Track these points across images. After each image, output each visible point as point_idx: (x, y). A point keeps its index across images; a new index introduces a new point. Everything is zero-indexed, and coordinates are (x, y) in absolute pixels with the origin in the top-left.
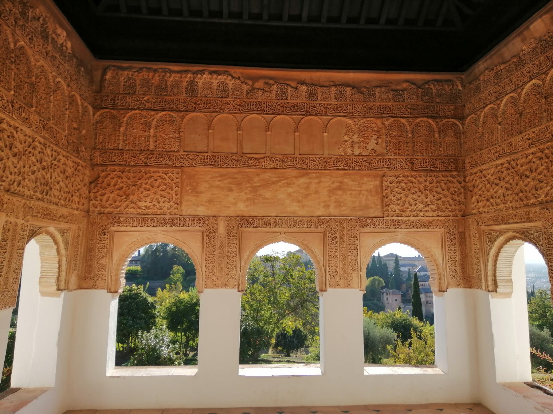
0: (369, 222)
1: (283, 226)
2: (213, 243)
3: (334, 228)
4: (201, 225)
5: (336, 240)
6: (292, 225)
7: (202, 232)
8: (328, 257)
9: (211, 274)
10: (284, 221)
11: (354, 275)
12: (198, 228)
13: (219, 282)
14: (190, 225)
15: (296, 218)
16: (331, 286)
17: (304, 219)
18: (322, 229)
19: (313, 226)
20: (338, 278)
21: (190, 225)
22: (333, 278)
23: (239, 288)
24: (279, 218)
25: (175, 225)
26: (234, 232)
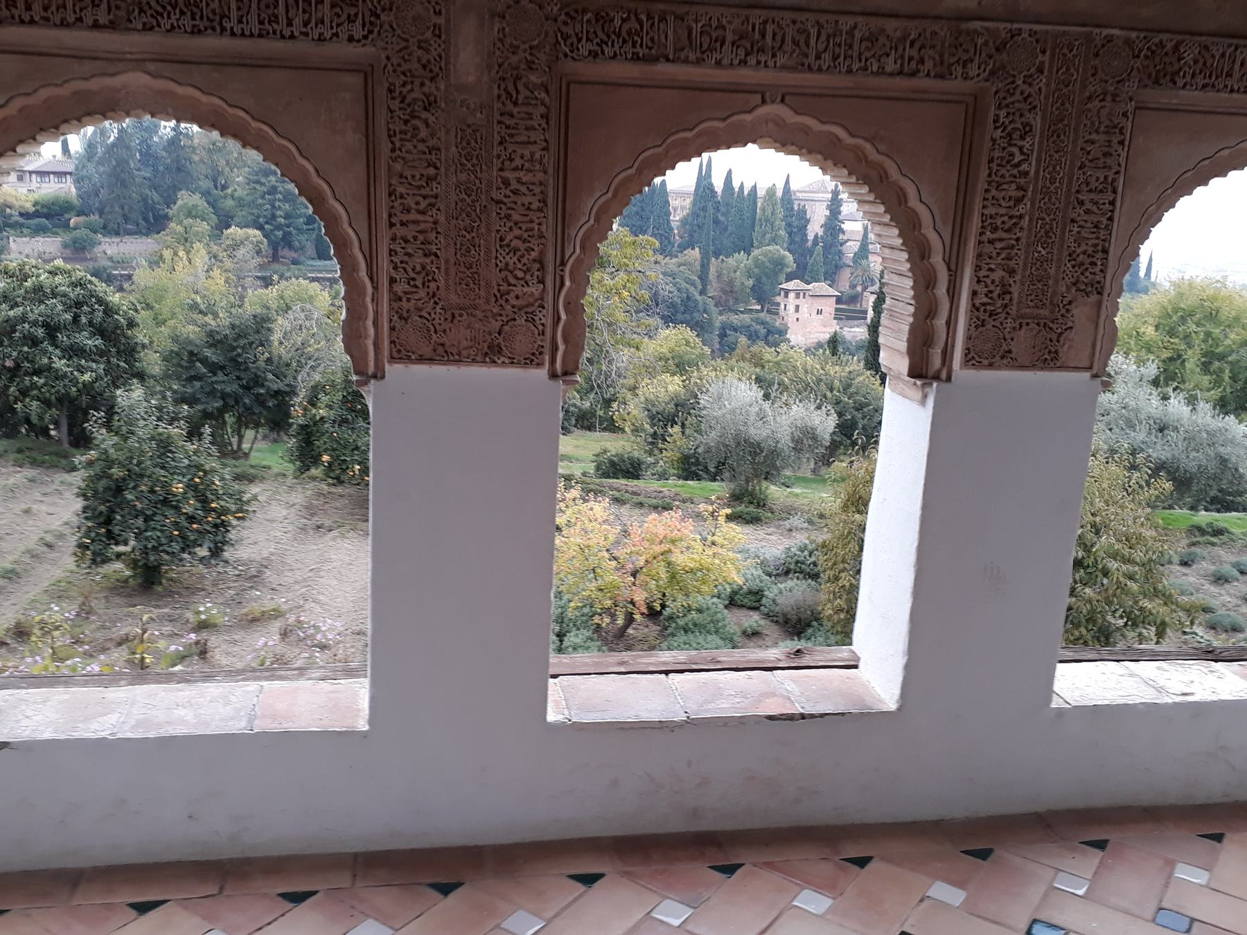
0: (1189, 58)
1: (781, 60)
2: (423, 133)
3: (1028, 80)
4: (358, 31)
5: (1026, 144)
6: (827, 56)
7: (366, 73)
8: (976, 222)
9: (422, 293)
10: (790, 32)
11: (1081, 312)
12: (342, 50)
13: (459, 335)
14: (297, 28)
15: (851, 21)
16: (971, 359)
17: (891, 25)
18: (968, 86)
19: (929, 64)
20: (1009, 324)
21: (297, 28)
22: (990, 323)
23: (553, 361)
24: (764, 14)
25: (217, 24)
26: (534, 78)
